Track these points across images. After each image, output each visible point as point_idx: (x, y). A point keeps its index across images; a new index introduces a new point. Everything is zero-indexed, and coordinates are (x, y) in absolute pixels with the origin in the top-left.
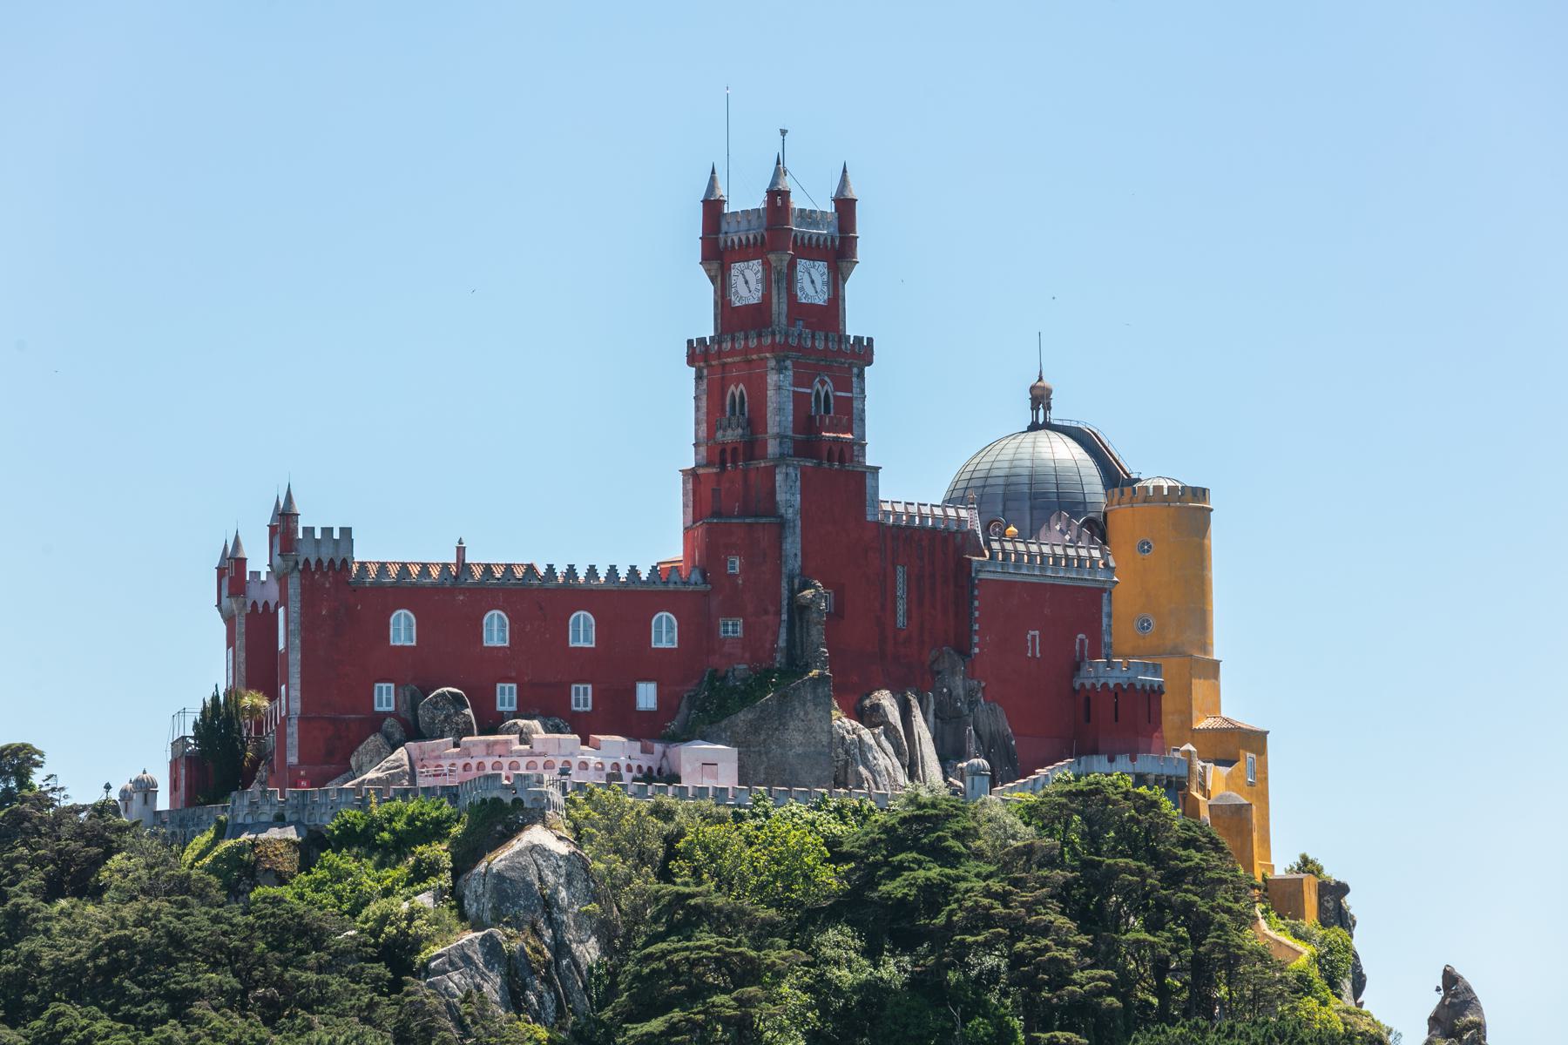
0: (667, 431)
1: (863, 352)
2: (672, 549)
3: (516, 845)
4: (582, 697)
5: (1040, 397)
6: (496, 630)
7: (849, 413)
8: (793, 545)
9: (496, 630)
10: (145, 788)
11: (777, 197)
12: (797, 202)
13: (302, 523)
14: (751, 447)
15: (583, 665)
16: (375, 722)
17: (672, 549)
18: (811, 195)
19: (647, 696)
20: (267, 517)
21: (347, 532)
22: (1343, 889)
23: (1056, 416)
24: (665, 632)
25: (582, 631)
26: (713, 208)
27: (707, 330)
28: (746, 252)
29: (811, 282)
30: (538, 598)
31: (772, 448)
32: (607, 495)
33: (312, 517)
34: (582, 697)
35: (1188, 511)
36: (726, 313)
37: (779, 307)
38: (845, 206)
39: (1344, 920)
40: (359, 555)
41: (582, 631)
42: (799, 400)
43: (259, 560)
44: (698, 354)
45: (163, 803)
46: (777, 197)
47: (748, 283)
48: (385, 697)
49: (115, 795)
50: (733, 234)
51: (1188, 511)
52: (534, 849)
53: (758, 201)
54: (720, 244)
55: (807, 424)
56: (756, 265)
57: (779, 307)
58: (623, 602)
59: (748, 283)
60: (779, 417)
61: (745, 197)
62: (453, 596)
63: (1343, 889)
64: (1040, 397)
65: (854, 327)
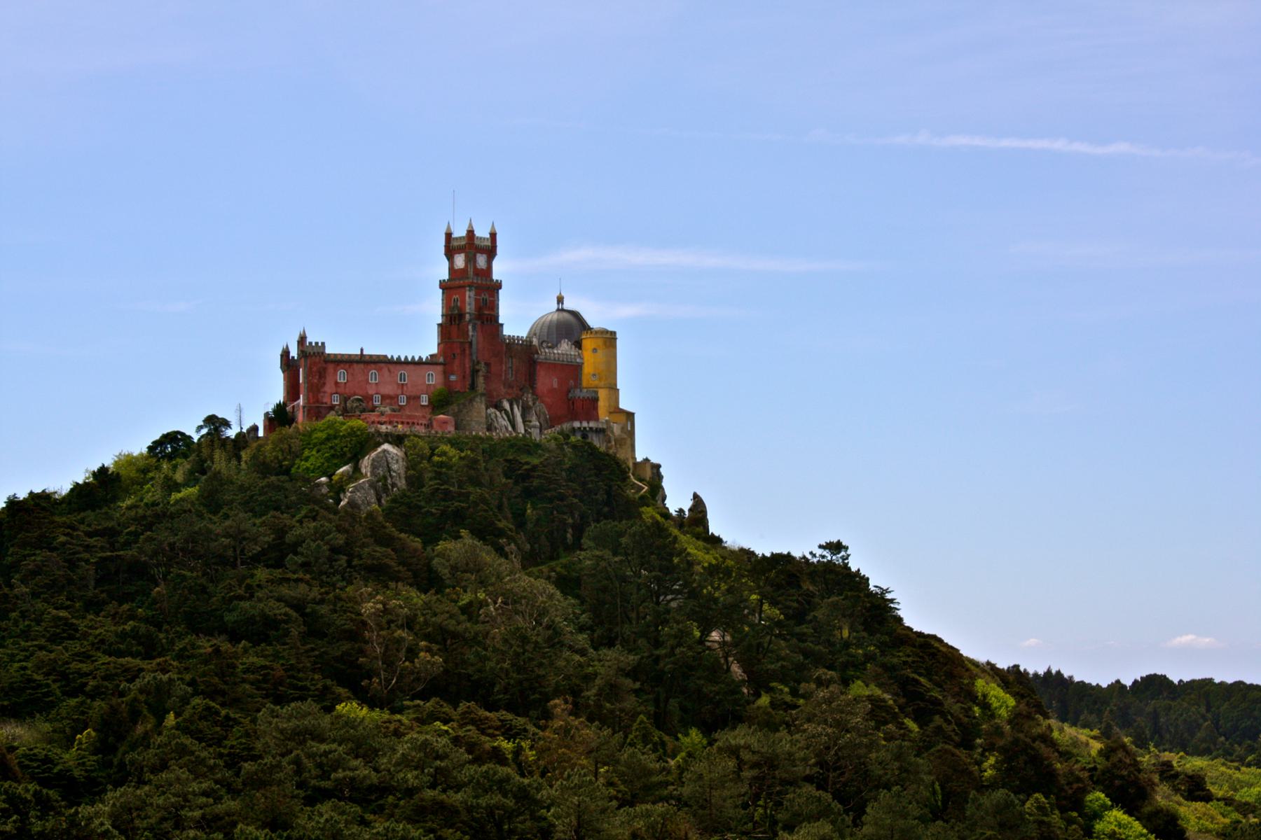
0: (434, 309)
1: (498, 286)
2: (435, 350)
3: (379, 450)
5: (560, 300)
7: (493, 306)
10: (254, 429)
11: (471, 233)
12: (478, 233)
13: (308, 340)
14: (461, 316)
16: (332, 408)
17: (435, 350)
18: (482, 232)
20: (297, 338)
21: (323, 344)
22: (659, 466)
23: (568, 305)
26: (449, 236)
27: (445, 275)
28: (460, 250)
29: (481, 261)
31: (468, 317)
33: (312, 339)
35: (609, 339)
36: (452, 270)
38: (493, 236)
39: (660, 477)
40: (328, 351)
42: (476, 300)
43: (294, 353)
45: (261, 433)
46: (471, 233)
47: (460, 261)
49: (244, 431)
50: (455, 244)
51: (609, 339)
52: (384, 451)
53: (463, 233)
54: (451, 250)
55: (479, 309)
56: (463, 255)
60: (469, 307)
61: (460, 232)
63: (659, 466)
64: (560, 300)
65: (495, 277)
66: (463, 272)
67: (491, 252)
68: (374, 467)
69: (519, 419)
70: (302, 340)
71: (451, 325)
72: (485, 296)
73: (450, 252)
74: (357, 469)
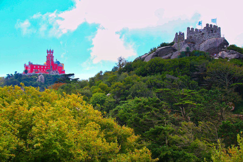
4: (42, 70)
5: (56, 60)
6: (38, 67)
7: (53, 59)
8: (51, 64)
9: (38, 67)
11: (50, 50)
15: (42, 69)
18: (52, 50)
19: (45, 70)
24: (45, 68)
25: (42, 67)
26: (47, 50)
29: (52, 54)
30: (40, 66)
32: (42, 62)
34: (42, 70)
36: (48, 55)
37: (50, 55)
38: (53, 51)
41: (42, 67)
44: (47, 56)
46: (50, 50)
48: (34, 70)
57: (50, 55)
58: (44, 66)
59: (49, 54)
61: (49, 50)
62: (37, 66)
64: (56, 60)
66: (49, 55)
67: (53, 53)
68: (40, 78)
69: (56, 73)
70: (30, 63)
71: (48, 62)
72: (52, 58)
73: (48, 52)
74: (38, 78)
